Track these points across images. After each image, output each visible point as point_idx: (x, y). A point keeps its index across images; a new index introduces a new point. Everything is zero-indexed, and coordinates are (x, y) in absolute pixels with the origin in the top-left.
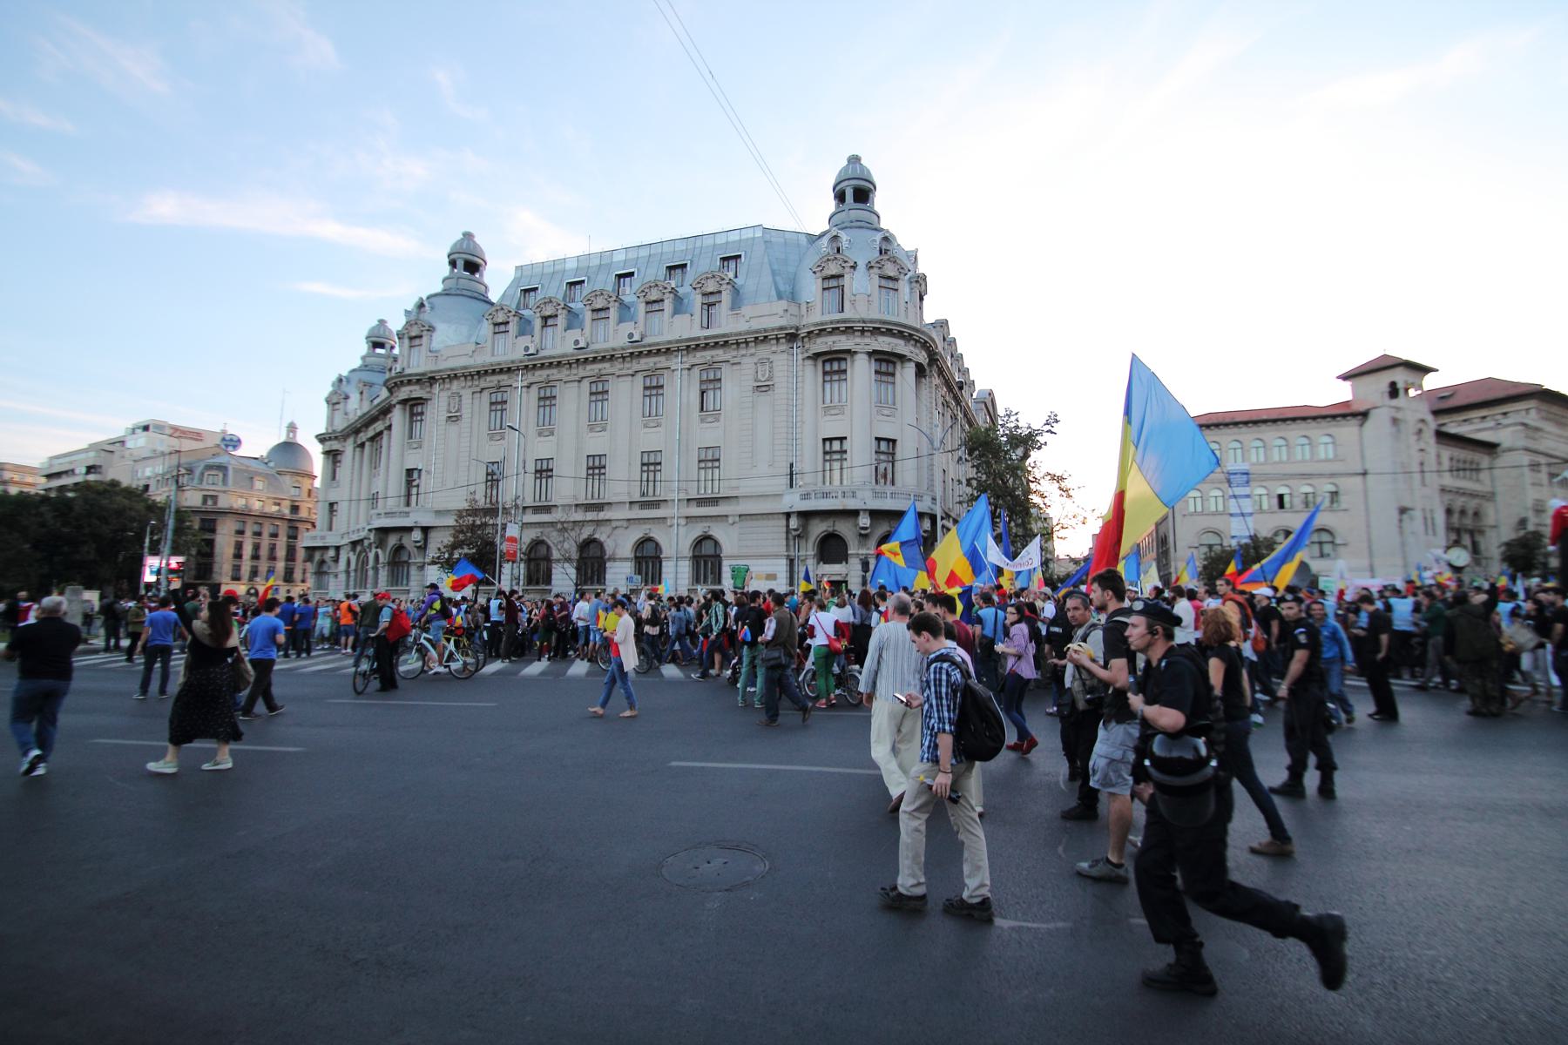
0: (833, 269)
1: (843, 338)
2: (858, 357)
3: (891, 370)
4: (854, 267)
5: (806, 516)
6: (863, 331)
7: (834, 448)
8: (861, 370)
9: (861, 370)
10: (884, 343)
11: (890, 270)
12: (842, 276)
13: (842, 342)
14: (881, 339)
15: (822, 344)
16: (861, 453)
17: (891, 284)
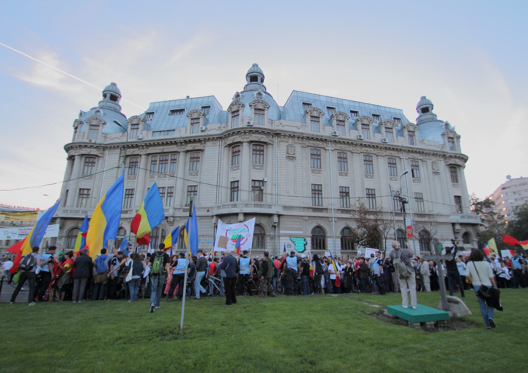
0: (235, 108)
1: (237, 136)
2: (244, 144)
3: (262, 149)
4: (243, 106)
6: (245, 133)
7: (234, 187)
8: (246, 151)
9: (246, 151)
10: (255, 137)
11: (260, 106)
12: (238, 111)
13: (237, 138)
14: (254, 135)
15: (230, 140)
16: (245, 186)
17: (261, 112)
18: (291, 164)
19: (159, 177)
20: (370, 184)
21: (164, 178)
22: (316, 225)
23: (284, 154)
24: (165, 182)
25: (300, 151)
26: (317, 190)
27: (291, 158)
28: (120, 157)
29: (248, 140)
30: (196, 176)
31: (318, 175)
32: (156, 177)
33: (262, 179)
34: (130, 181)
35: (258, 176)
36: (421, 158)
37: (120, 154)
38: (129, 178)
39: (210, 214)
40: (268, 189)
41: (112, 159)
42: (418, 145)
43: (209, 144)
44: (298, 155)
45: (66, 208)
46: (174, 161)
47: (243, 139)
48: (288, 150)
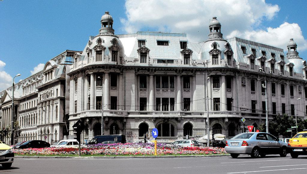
5: (211, 119)
6: (224, 71)
15: (213, 73)
18: (244, 89)
19: (163, 91)
20: (274, 100)
21: (167, 92)
22: (254, 123)
23: (241, 84)
24: (168, 95)
25: (247, 81)
26: (254, 103)
27: (244, 86)
28: (135, 75)
29: (226, 75)
30: (188, 92)
31: (254, 95)
32: (161, 90)
33: (231, 98)
34: (142, 92)
35: (230, 96)
36: (294, 84)
37: (135, 73)
38: (141, 90)
39: (205, 116)
40: (234, 104)
41: (131, 77)
42: (294, 77)
43: (198, 73)
44: (246, 84)
45: (91, 110)
46: (172, 82)
47: (223, 73)
48: (242, 81)
